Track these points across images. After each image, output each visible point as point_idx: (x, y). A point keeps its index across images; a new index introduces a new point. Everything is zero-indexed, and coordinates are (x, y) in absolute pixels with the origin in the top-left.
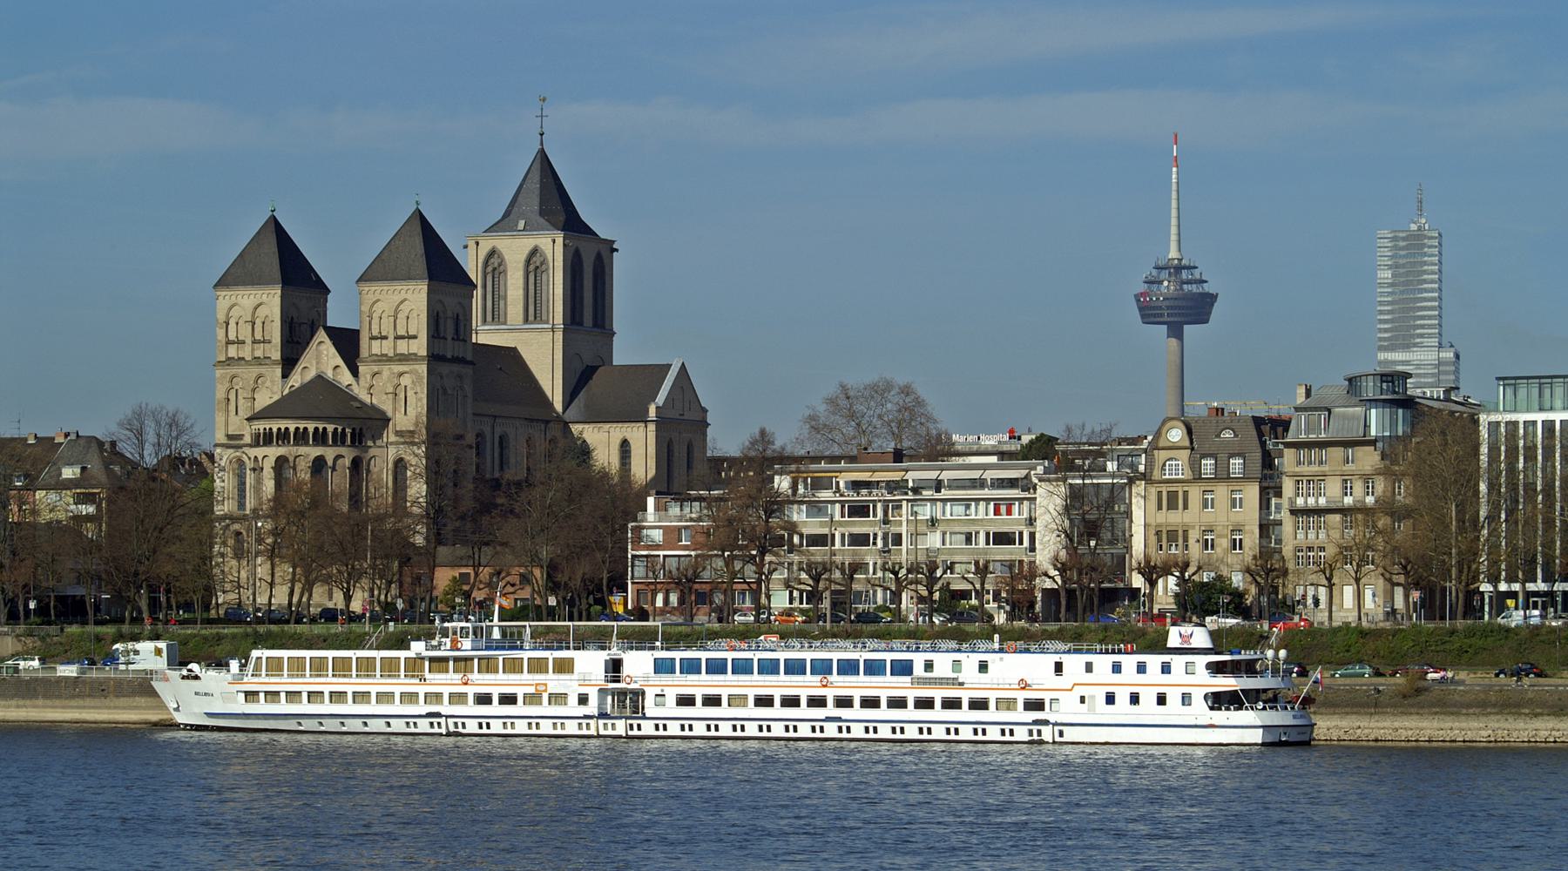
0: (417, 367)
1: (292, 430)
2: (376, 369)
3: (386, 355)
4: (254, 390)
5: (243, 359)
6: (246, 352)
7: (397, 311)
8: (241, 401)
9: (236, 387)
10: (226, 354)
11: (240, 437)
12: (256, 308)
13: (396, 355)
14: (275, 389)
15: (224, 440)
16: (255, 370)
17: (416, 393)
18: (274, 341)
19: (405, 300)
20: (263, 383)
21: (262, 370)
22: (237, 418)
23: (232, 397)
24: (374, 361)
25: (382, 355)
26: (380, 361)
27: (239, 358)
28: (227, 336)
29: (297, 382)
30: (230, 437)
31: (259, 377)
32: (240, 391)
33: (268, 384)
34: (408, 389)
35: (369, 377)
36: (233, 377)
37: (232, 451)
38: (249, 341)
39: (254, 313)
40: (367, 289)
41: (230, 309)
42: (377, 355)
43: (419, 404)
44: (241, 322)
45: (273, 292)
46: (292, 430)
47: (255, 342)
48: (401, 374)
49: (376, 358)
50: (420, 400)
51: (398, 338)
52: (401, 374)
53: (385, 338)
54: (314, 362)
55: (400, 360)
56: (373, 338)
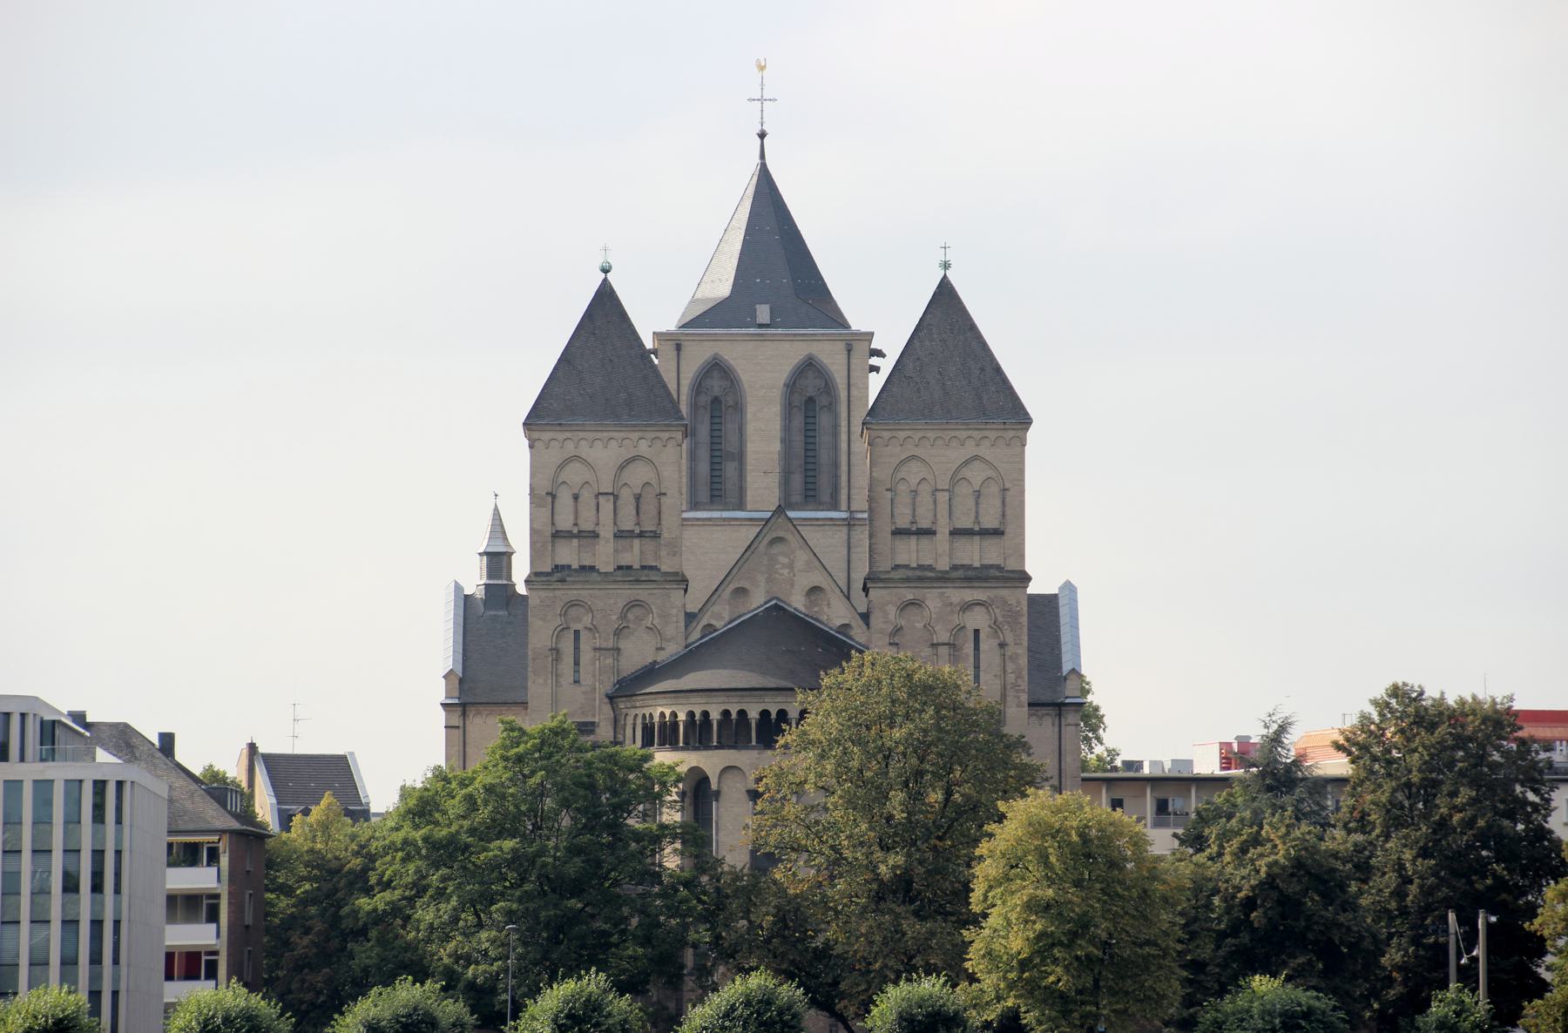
0: (1003, 592)
1: (715, 716)
2: (909, 595)
3: (930, 568)
4: (618, 633)
5: (592, 568)
6: (604, 555)
7: (956, 479)
8: (586, 656)
9: (575, 626)
10: (553, 559)
12: (622, 467)
13: (955, 568)
14: (670, 631)
17: (1002, 645)
18: (665, 535)
19: (976, 458)
20: (639, 619)
21: (641, 593)
23: (567, 646)
24: (908, 580)
25: (921, 567)
26: (920, 579)
27: (583, 568)
28: (553, 524)
29: (719, 617)
31: (635, 604)
32: (584, 636)
33: (653, 619)
34: (982, 636)
35: (892, 611)
38: (606, 532)
39: (617, 476)
40: (886, 435)
41: (561, 466)
42: (907, 567)
43: (1010, 667)
44: (587, 496)
45: (665, 435)
46: (715, 716)
47: (620, 535)
48: (967, 607)
49: (910, 573)
50: (1014, 658)
51: (956, 533)
52: (967, 607)
53: (930, 532)
54: (761, 579)
55: (967, 579)
56: (898, 532)
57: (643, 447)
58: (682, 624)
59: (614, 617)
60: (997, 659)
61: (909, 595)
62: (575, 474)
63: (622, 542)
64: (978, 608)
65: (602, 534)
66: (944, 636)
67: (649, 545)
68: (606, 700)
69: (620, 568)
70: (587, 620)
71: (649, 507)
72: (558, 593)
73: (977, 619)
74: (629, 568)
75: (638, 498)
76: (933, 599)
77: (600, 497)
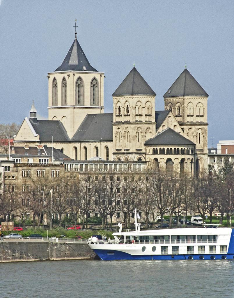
6: (143, 119)
8: (140, 137)
11: (141, 150)
15: (135, 151)
16: (147, 126)
17: (204, 136)
20: (148, 130)
21: (149, 126)
22: (139, 143)
29: (160, 130)
30: (137, 150)
31: (148, 128)
32: (140, 133)
34: (200, 134)
36: (139, 128)
37: (138, 155)
38: (144, 115)
44: (140, 108)
57: (149, 99)
58: (155, 131)
59: (145, 130)
60: (203, 139)
61: (190, 127)
62: (139, 104)
63: (146, 117)
64: (200, 129)
65: (143, 115)
66: (195, 134)
67: (150, 117)
68: (144, 145)
69: (145, 121)
70: (141, 130)
71: (150, 110)
72: (137, 125)
73: (200, 131)
74: (147, 121)
75: (148, 109)
76: (193, 127)
77: (143, 108)
